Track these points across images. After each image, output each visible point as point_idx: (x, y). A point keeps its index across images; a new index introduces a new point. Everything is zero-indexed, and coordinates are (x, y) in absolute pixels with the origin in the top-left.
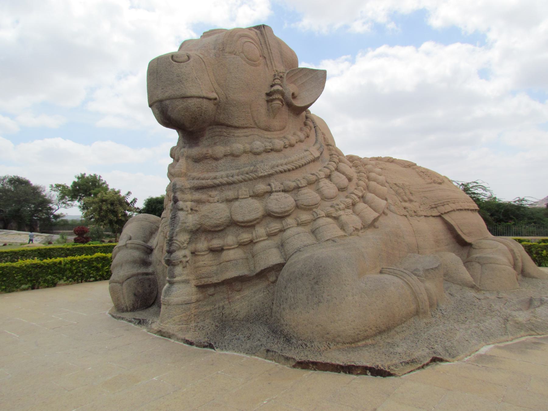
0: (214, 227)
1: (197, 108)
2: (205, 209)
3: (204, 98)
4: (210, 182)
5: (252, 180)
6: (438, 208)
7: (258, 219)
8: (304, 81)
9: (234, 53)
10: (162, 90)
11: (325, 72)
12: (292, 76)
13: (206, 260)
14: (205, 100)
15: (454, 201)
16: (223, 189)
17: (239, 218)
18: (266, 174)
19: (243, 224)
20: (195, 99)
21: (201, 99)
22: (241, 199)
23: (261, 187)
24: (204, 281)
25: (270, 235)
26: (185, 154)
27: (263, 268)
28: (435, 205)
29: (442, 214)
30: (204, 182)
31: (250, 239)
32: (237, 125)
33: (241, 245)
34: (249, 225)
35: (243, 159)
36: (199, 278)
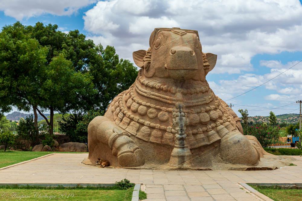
0: (196, 124)
2: (192, 116)
4: (191, 104)
11: (217, 55)
13: (192, 138)
17: (203, 120)
19: (203, 123)
24: (193, 147)
25: (213, 128)
31: (206, 130)
32: (196, 79)
33: (204, 132)
34: (205, 124)
35: (200, 95)
36: (191, 145)
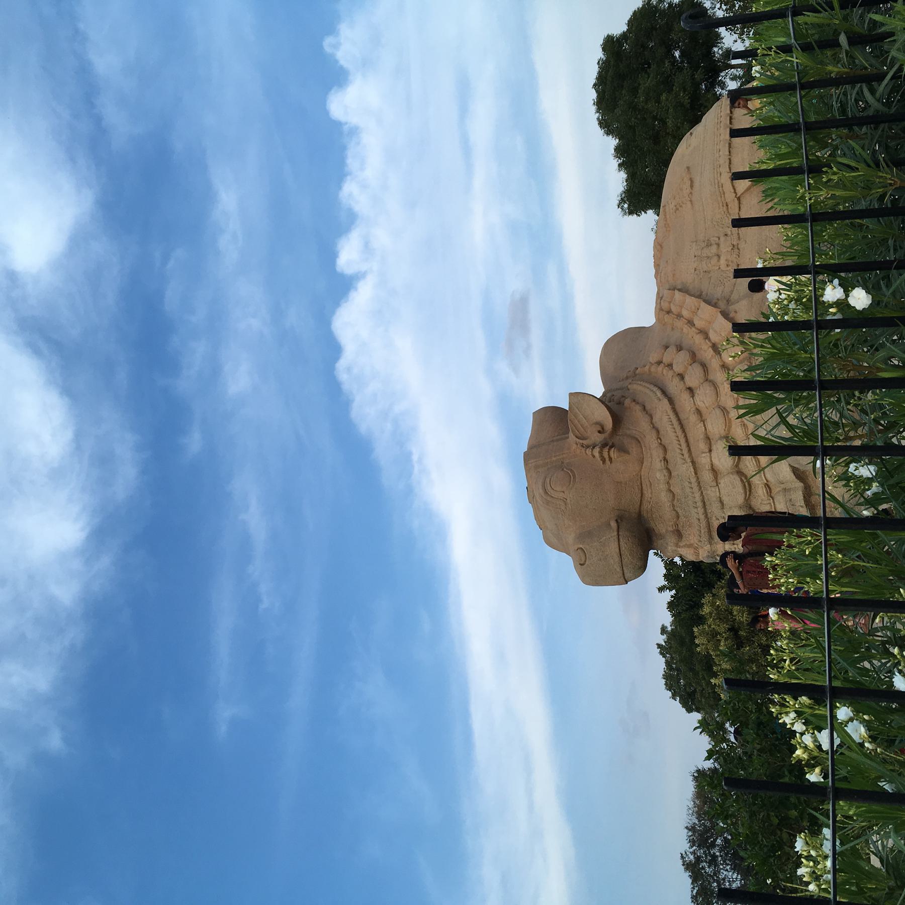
1: (629, 540)
3: (618, 535)
5: (699, 482)
6: (728, 200)
7: (742, 480)
8: (582, 417)
9: (565, 500)
10: (614, 573)
11: (571, 394)
12: (578, 431)
14: (620, 533)
15: (717, 173)
16: (710, 511)
18: (692, 468)
19: (748, 493)
20: (620, 543)
21: (620, 537)
22: (720, 495)
23: (707, 476)
26: (674, 548)
27: (794, 477)
28: (723, 206)
29: (736, 197)
30: (702, 532)
35: (677, 490)
